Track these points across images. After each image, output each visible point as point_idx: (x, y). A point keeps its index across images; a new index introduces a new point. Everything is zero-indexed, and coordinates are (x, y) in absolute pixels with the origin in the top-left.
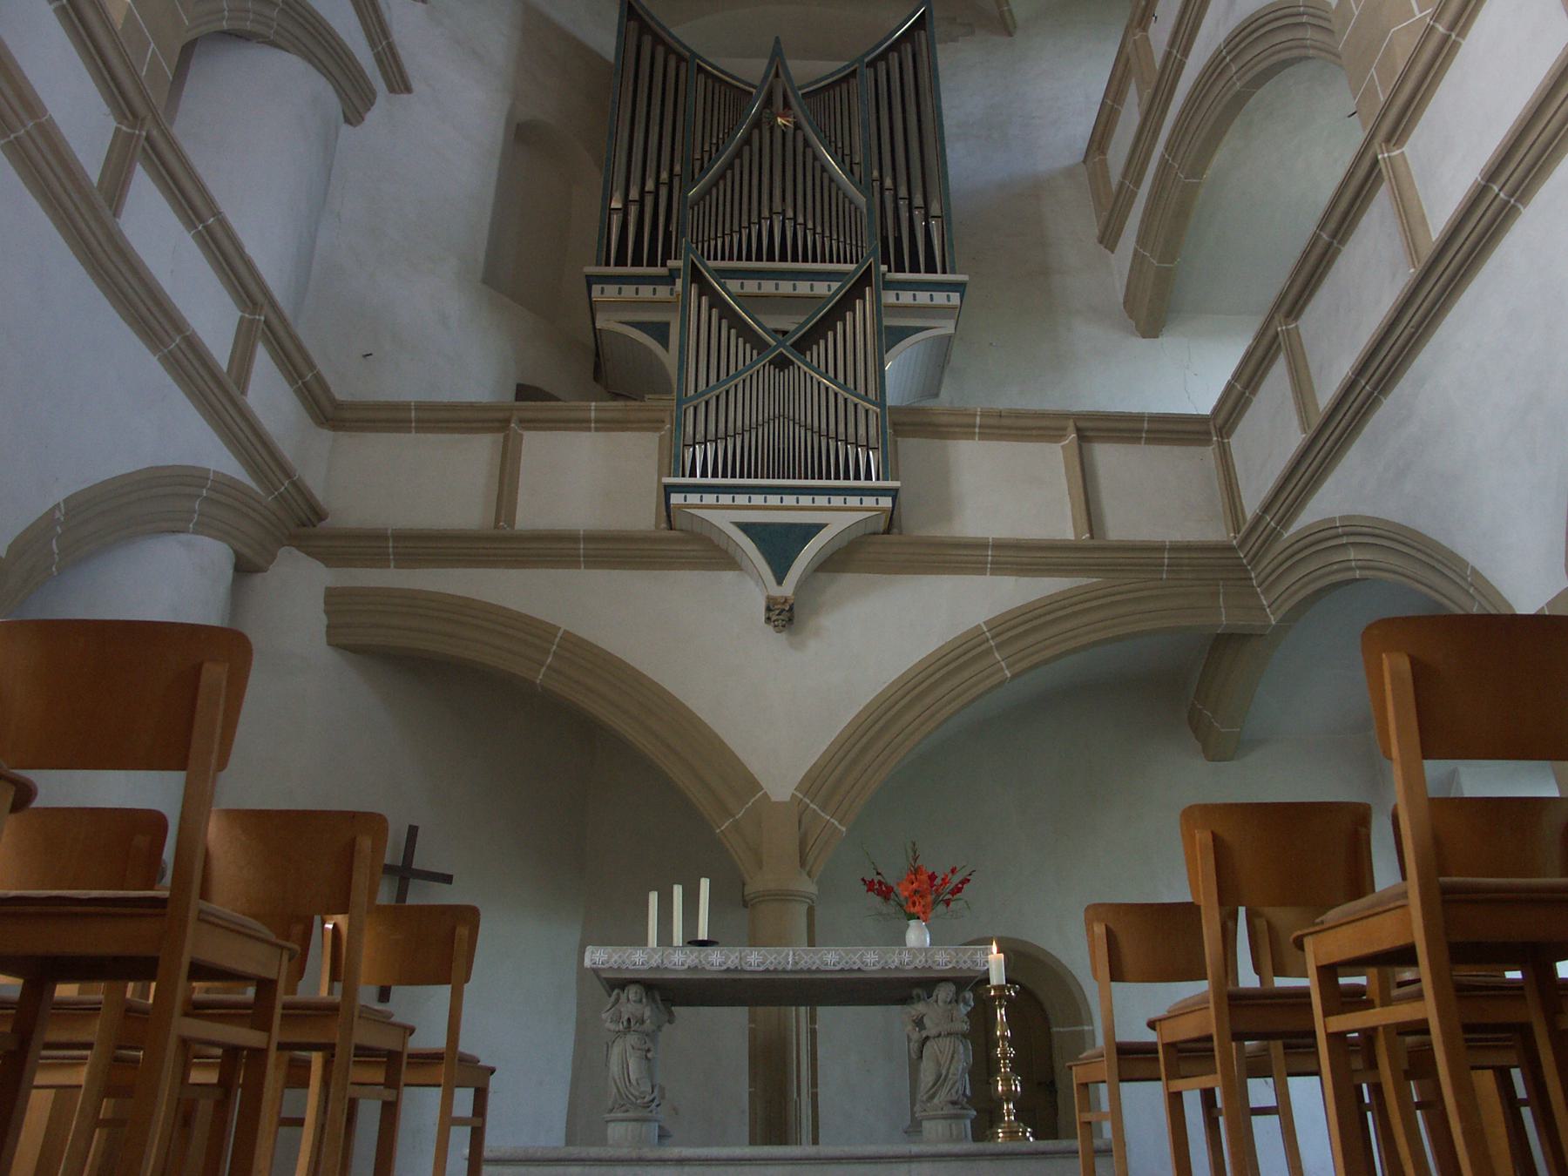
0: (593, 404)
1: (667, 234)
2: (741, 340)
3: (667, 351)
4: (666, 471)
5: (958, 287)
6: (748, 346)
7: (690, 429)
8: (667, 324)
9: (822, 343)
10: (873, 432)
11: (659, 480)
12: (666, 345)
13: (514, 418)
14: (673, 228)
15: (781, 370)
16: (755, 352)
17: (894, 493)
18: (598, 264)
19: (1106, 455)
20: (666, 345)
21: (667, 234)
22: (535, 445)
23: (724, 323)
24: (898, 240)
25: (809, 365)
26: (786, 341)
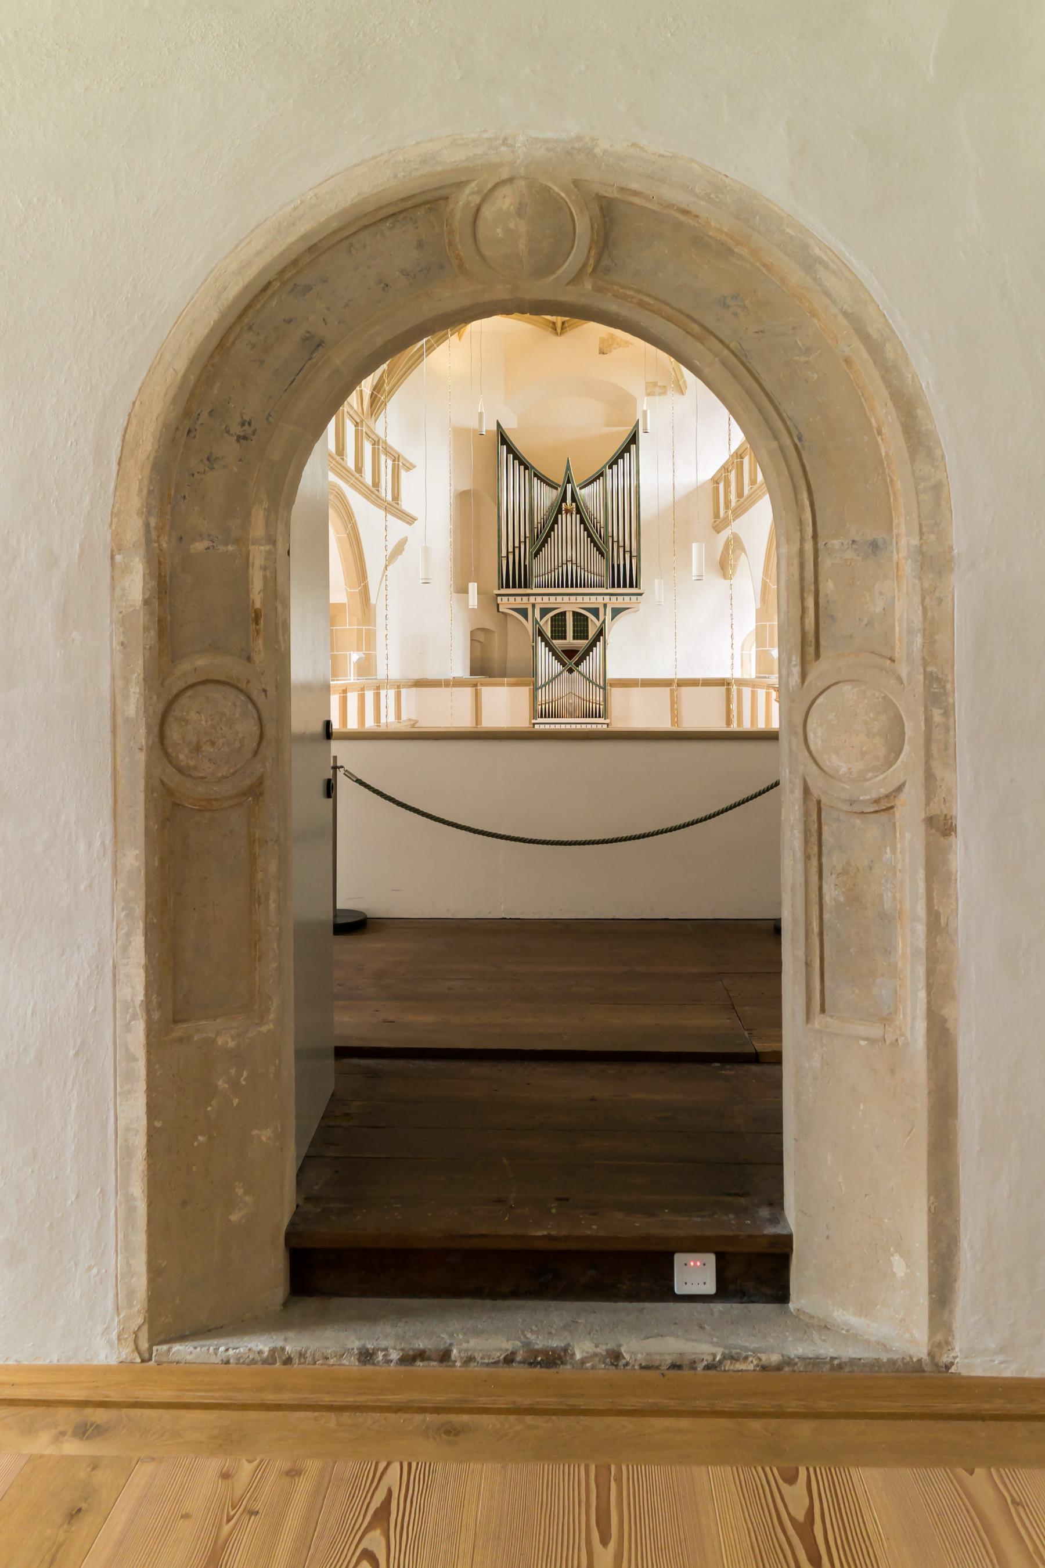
0: (506, 679)
1: (525, 566)
2: (556, 661)
3: (527, 621)
4: (532, 718)
5: (641, 594)
6: (559, 664)
7: (540, 700)
8: (526, 609)
9: (585, 661)
10: (601, 699)
11: (530, 721)
12: (526, 618)
13: (479, 683)
14: (527, 563)
15: (571, 674)
16: (561, 666)
17: (608, 724)
18: (499, 589)
19: (684, 690)
20: (526, 618)
21: (525, 566)
22: (487, 692)
23: (551, 653)
24: (619, 566)
25: (580, 673)
26: (572, 662)
